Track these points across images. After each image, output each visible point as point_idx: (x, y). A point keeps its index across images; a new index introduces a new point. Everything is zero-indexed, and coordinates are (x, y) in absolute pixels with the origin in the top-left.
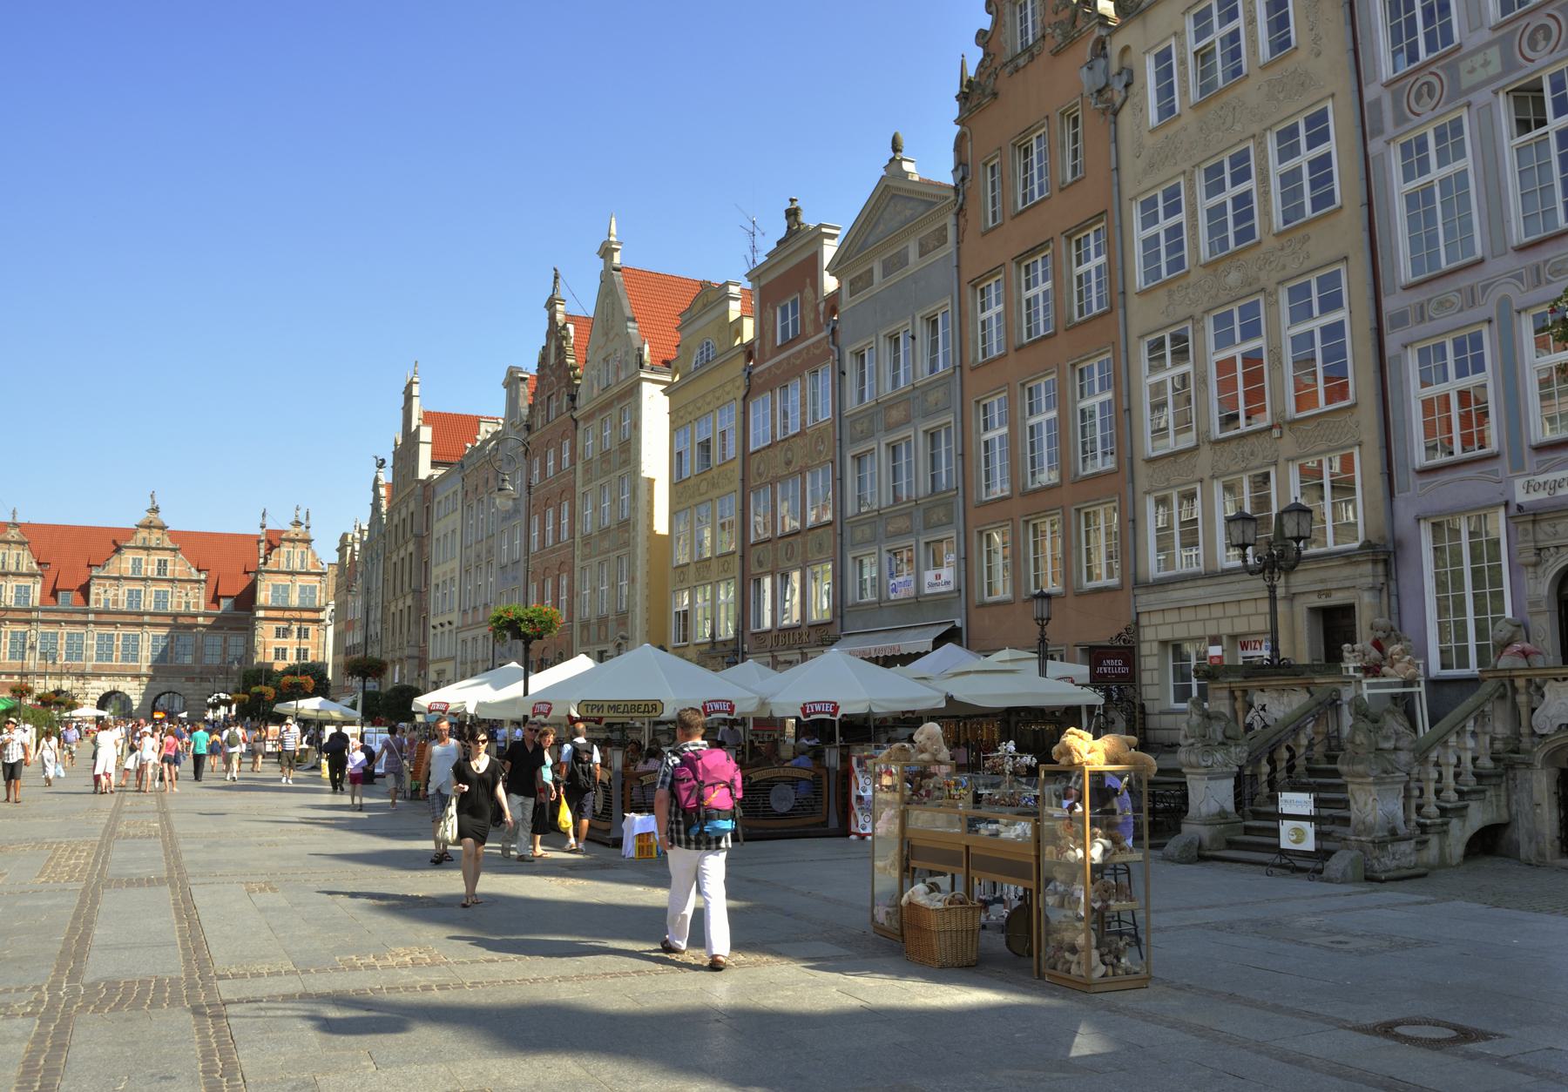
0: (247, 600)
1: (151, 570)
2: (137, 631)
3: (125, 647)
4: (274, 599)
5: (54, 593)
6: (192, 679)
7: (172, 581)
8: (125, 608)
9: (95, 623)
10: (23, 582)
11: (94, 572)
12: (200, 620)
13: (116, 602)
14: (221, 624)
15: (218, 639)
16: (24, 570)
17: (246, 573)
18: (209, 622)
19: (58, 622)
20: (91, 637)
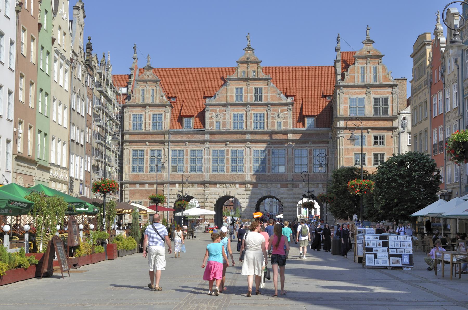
0: (327, 118)
1: (250, 97)
2: (241, 147)
3: (234, 160)
4: (352, 110)
5: (180, 120)
6: (285, 186)
7: (266, 105)
8: (231, 128)
9: (211, 142)
10: (158, 111)
11: (208, 101)
12: (290, 136)
13: (225, 124)
14: (306, 139)
15: (303, 152)
16: (158, 102)
17: (324, 96)
18: (297, 137)
19: (183, 142)
20: (208, 152)
